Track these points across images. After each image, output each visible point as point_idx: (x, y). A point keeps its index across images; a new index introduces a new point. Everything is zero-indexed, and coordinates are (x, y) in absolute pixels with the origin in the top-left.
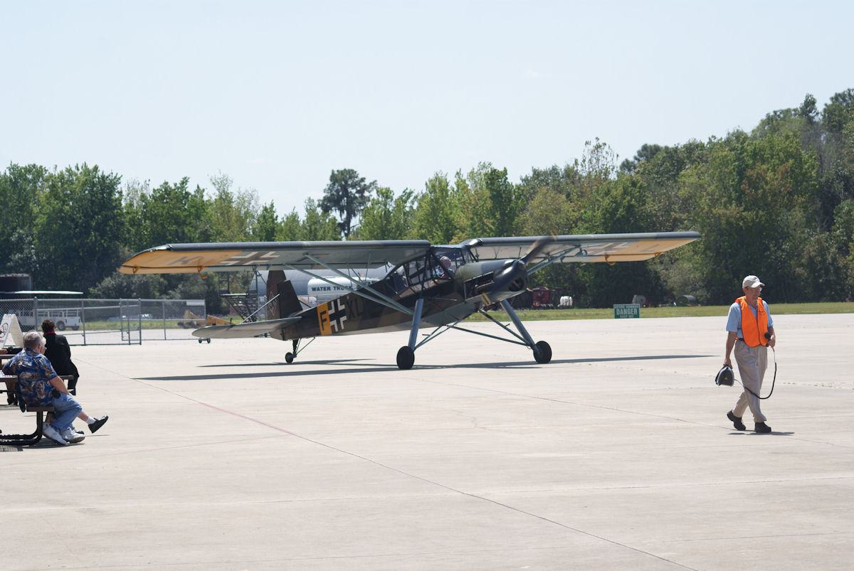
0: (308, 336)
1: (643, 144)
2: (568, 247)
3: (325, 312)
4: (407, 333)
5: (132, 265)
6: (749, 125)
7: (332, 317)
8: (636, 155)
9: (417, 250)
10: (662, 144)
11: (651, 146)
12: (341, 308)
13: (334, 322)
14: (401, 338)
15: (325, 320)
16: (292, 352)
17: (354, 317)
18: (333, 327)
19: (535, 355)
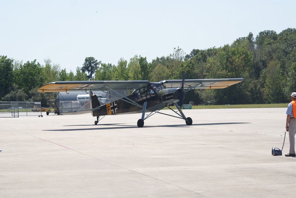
0: (102, 115)
1: (193, 49)
2: (197, 83)
3: (109, 106)
4: (141, 114)
5: (42, 89)
6: (230, 42)
7: (112, 108)
8: (191, 53)
9: (144, 84)
10: (200, 49)
11: (196, 50)
12: (115, 105)
13: (113, 110)
14: (139, 116)
15: (109, 109)
16: (97, 120)
17: (120, 108)
18: (112, 112)
19: (186, 122)
